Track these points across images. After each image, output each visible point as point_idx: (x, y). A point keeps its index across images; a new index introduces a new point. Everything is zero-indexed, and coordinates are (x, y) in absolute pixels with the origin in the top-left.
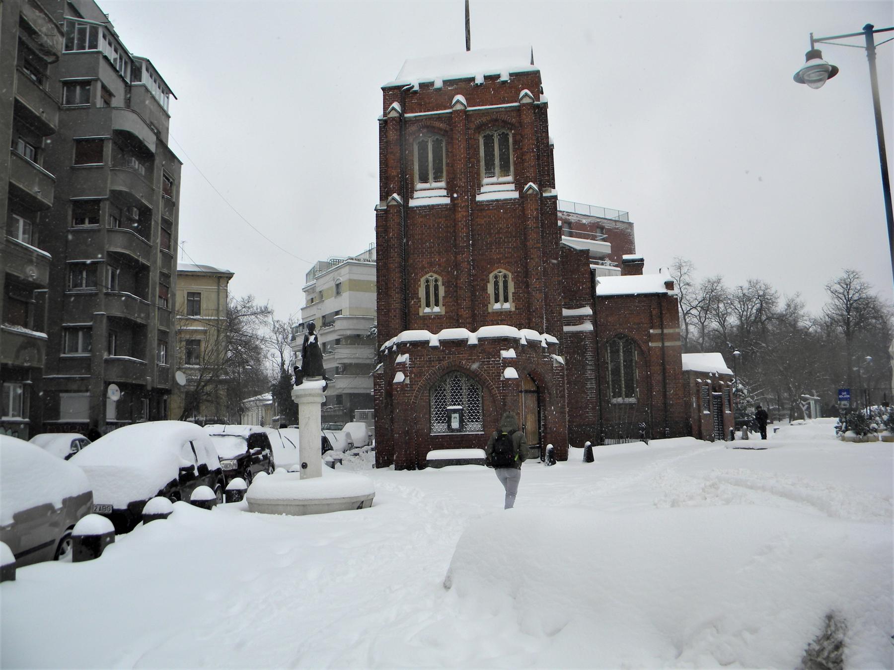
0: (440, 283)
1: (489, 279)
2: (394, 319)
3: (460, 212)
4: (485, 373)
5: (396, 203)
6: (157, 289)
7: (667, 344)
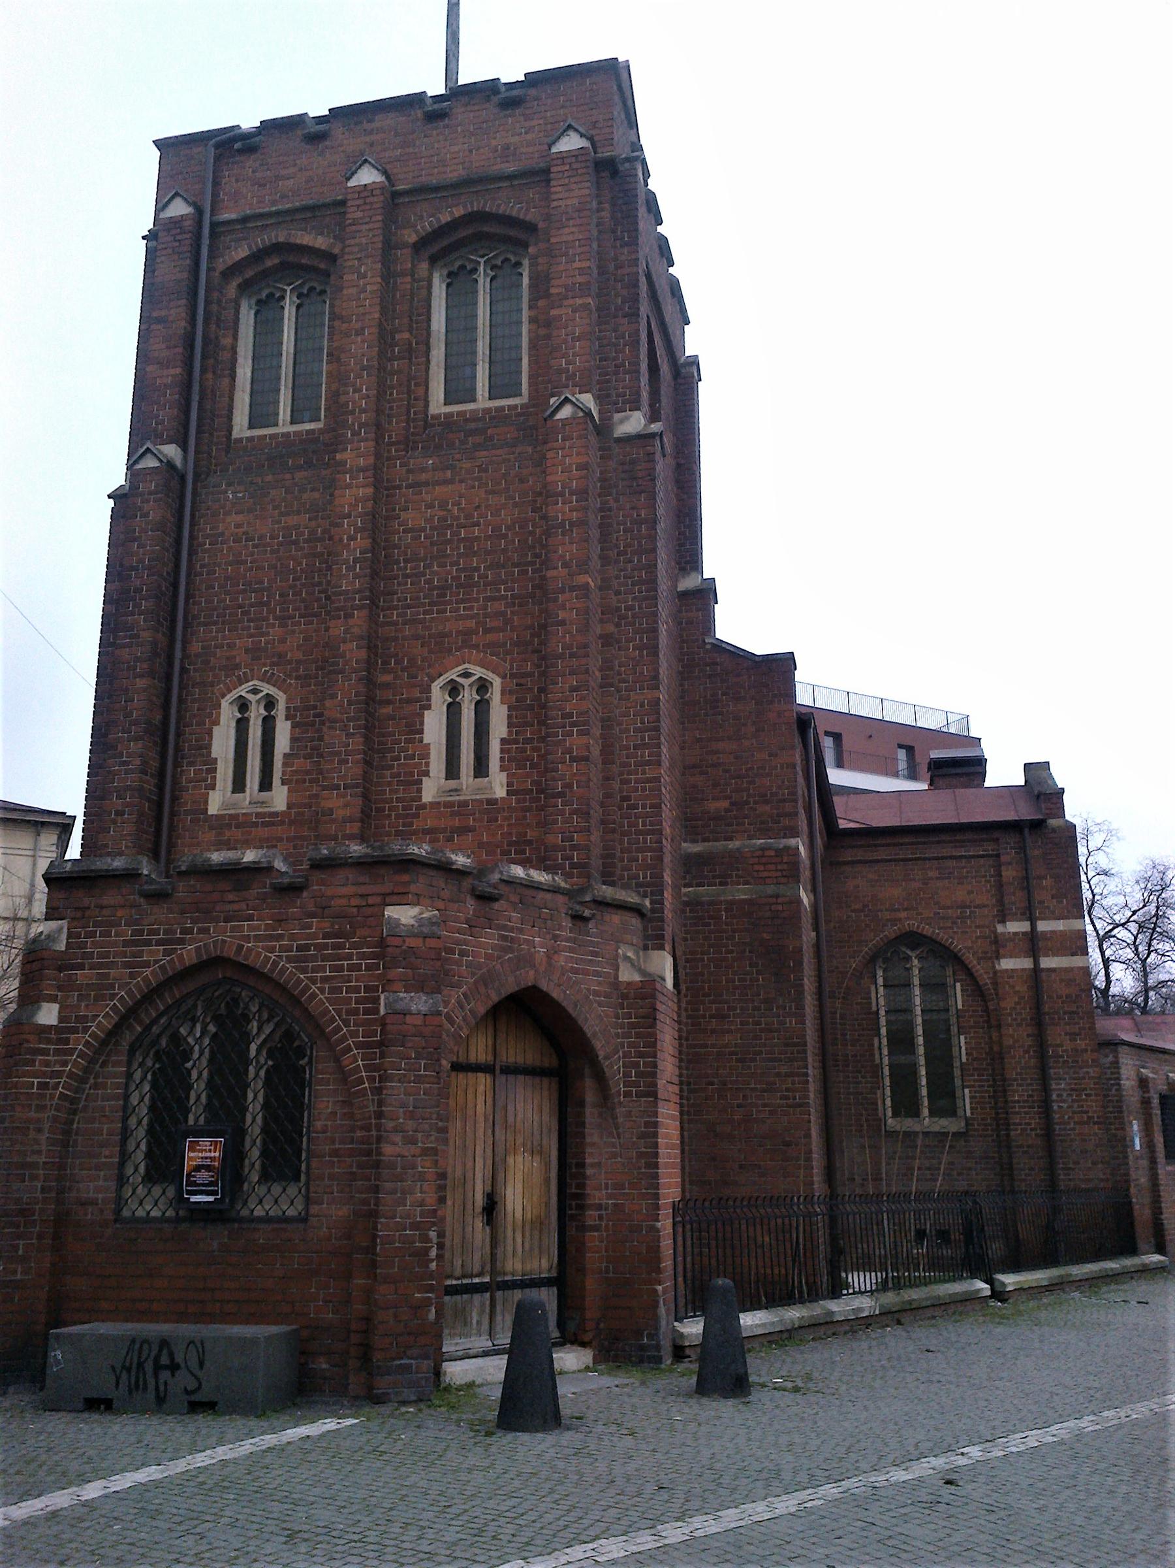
1: (429, 699)
2: (114, 822)
3: (349, 486)
4: (322, 991)
5: (157, 464)
7: (1047, 962)
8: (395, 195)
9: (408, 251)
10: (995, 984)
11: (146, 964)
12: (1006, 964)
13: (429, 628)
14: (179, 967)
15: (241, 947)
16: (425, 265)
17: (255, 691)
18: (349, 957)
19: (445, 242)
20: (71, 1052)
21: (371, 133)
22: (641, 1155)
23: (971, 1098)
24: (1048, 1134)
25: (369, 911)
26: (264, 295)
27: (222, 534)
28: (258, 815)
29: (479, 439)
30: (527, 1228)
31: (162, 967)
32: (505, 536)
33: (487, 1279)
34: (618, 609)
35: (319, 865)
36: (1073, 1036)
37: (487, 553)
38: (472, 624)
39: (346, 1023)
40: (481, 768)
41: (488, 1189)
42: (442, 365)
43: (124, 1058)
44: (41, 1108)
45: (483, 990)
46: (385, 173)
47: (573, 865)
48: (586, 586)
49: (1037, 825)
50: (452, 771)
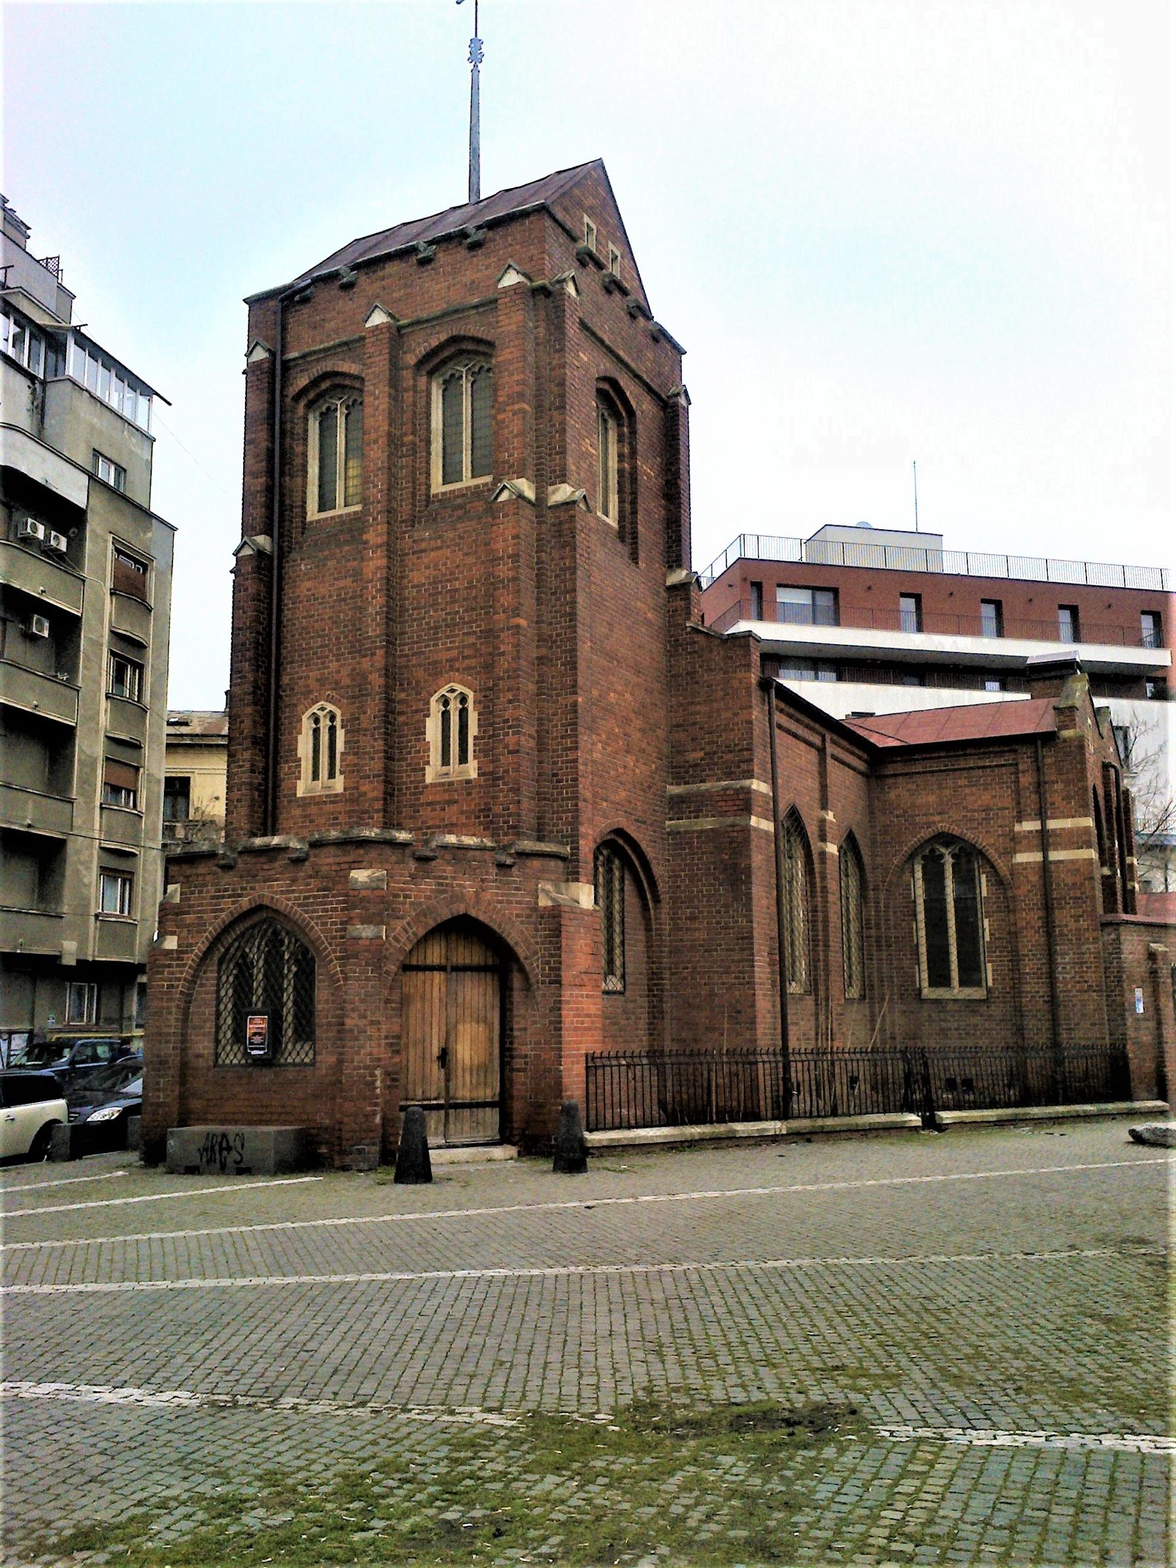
1: (429, 710)
3: (372, 559)
6: (99, 771)
7: (1054, 856)
8: (399, 329)
9: (410, 371)
10: (1011, 874)
11: (222, 910)
12: (1021, 858)
14: (241, 911)
16: (424, 379)
17: (323, 709)
19: (436, 360)
20: (184, 965)
21: (383, 279)
22: (551, 1022)
23: (993, 970)
24: (1053, 1001)
26: (324, 409)
27: (299, 597)
28: (327, 796)
29: (460, 512)
30: (475, 1073)
31: (231, 912)
32: (475, 587)
33: (442, 1102)
34: (551, 636)
35: (315, 845)
36: (1077, 918)
37: (465, 599)
38: (455, 653)
39: (330, 944)
41: (443, 1045)
42: (441, 454)
43: (215, 968)
44: (171, 1000)
45: (423, 919)
46: (390, 315)
47: (509, 827)
48: (518, 626)
49: (1048, 738)
50: (445, 761)
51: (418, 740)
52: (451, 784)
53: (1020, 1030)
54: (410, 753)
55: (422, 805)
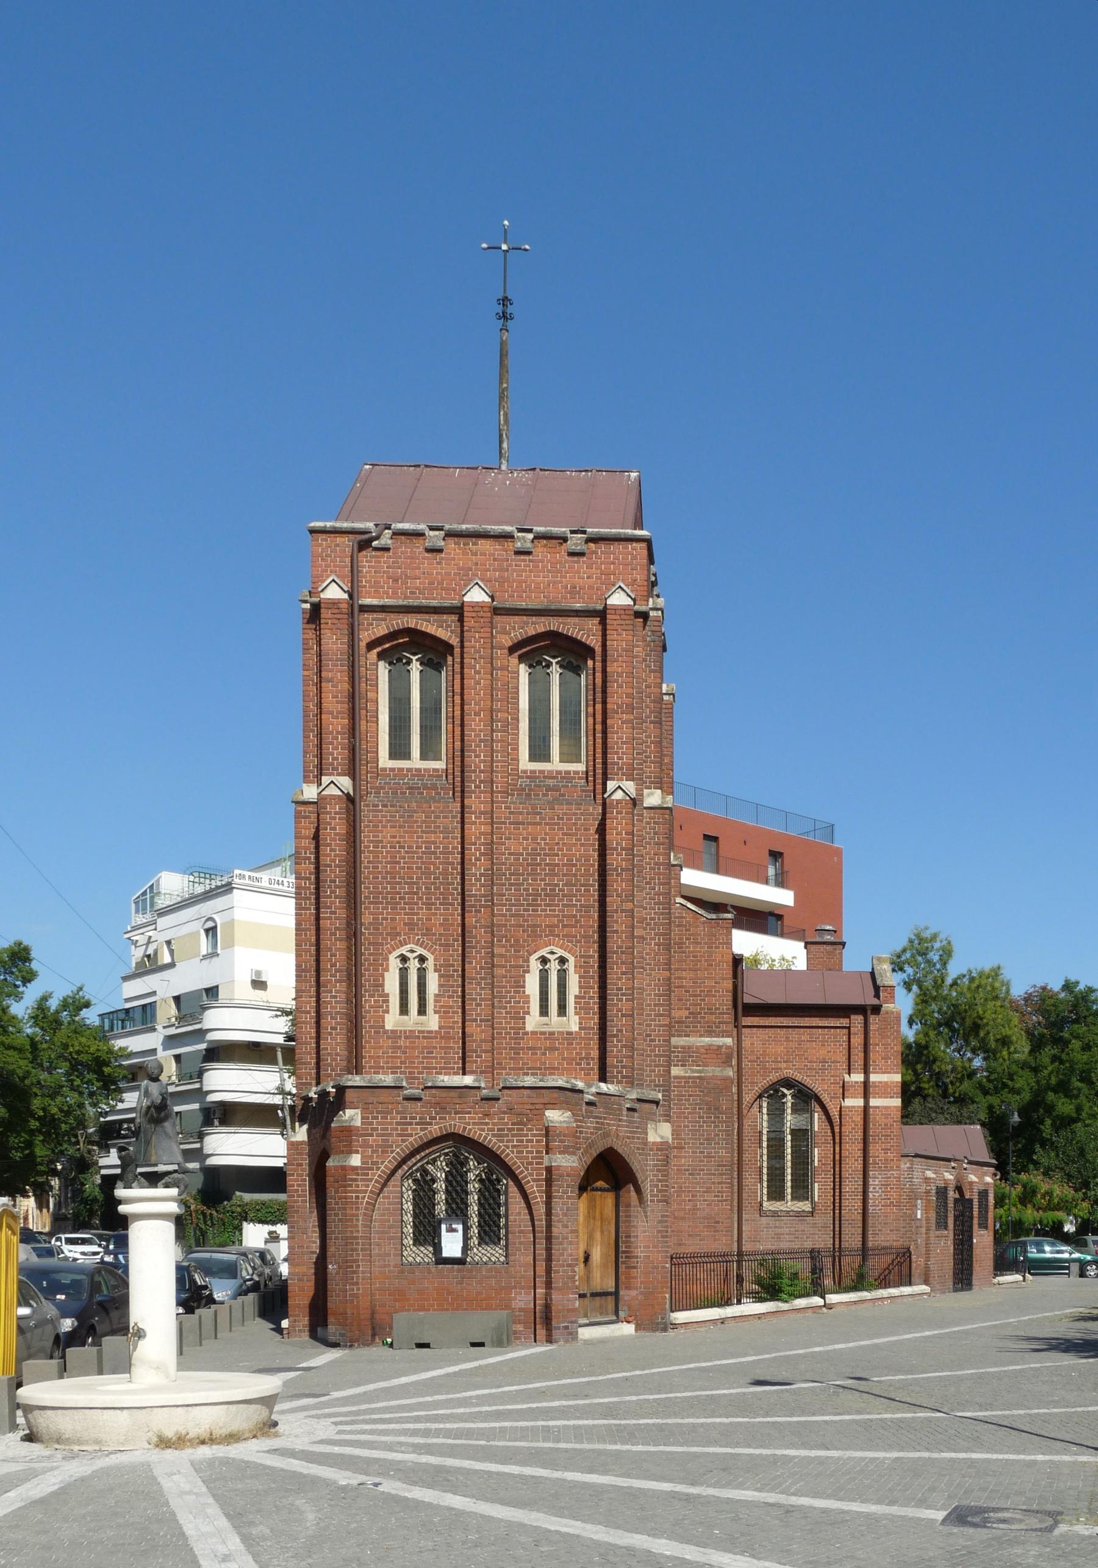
0: (430, 964)
1: (528, 966)
4: (513, 1152)
13: (527, 921)
14: (430, 1138)
15: (465, 1128)
18: (527, 1135)
22: (659, 1231)
23: (819, 1189)
25: (536, 1112)
28: (419, 1032)
32: (575, 865)
37: (564, 875)
39: (527, 1169)
40: (562, 1009)
47: (623, 1077)
50: (544, 1011)
51: (519, 992)
52: (552, 1033)
53: (838, 1234)
54: (510, 1002)
55: (523, 1049)
